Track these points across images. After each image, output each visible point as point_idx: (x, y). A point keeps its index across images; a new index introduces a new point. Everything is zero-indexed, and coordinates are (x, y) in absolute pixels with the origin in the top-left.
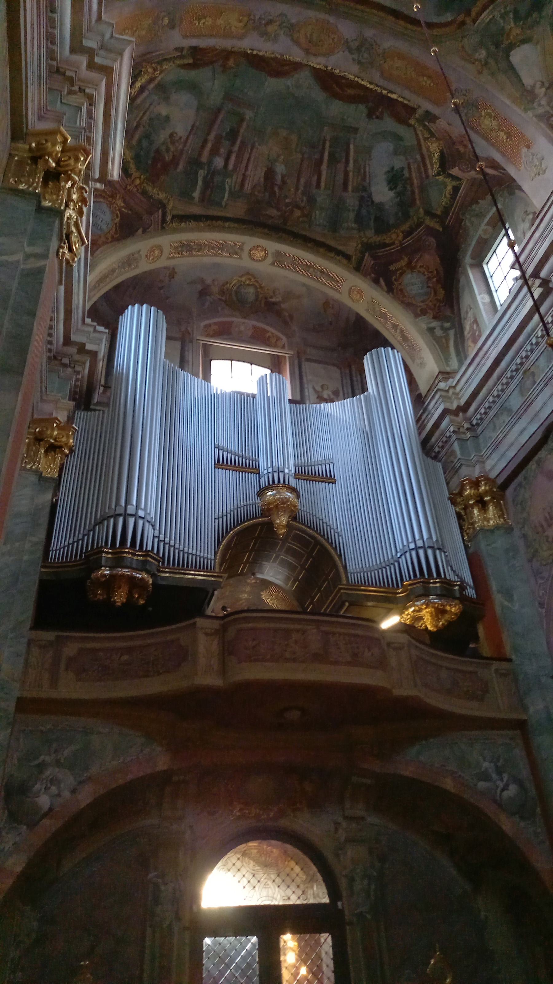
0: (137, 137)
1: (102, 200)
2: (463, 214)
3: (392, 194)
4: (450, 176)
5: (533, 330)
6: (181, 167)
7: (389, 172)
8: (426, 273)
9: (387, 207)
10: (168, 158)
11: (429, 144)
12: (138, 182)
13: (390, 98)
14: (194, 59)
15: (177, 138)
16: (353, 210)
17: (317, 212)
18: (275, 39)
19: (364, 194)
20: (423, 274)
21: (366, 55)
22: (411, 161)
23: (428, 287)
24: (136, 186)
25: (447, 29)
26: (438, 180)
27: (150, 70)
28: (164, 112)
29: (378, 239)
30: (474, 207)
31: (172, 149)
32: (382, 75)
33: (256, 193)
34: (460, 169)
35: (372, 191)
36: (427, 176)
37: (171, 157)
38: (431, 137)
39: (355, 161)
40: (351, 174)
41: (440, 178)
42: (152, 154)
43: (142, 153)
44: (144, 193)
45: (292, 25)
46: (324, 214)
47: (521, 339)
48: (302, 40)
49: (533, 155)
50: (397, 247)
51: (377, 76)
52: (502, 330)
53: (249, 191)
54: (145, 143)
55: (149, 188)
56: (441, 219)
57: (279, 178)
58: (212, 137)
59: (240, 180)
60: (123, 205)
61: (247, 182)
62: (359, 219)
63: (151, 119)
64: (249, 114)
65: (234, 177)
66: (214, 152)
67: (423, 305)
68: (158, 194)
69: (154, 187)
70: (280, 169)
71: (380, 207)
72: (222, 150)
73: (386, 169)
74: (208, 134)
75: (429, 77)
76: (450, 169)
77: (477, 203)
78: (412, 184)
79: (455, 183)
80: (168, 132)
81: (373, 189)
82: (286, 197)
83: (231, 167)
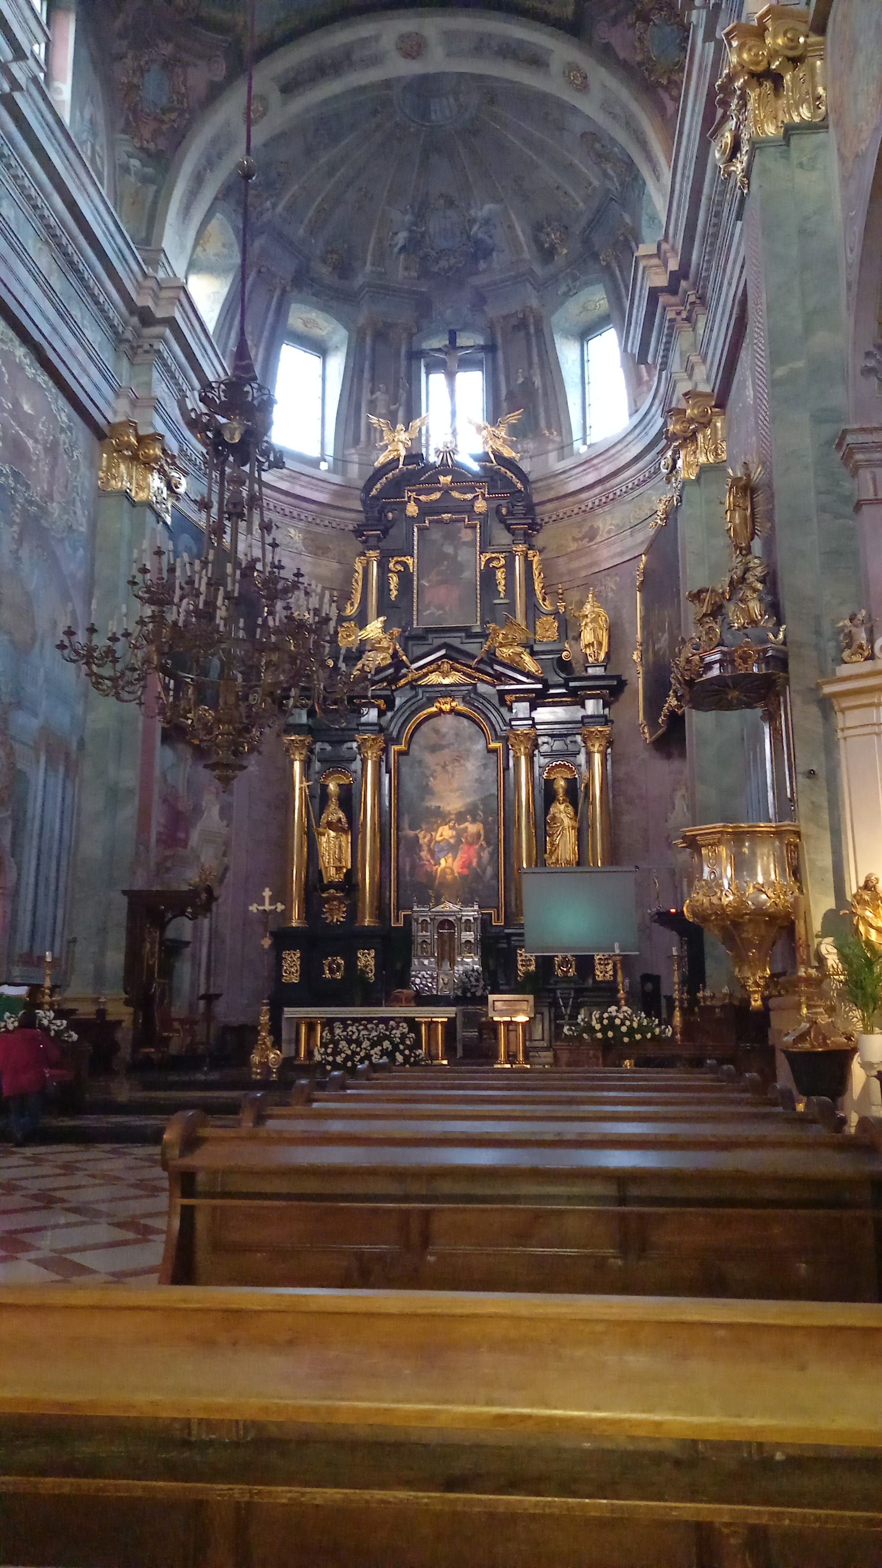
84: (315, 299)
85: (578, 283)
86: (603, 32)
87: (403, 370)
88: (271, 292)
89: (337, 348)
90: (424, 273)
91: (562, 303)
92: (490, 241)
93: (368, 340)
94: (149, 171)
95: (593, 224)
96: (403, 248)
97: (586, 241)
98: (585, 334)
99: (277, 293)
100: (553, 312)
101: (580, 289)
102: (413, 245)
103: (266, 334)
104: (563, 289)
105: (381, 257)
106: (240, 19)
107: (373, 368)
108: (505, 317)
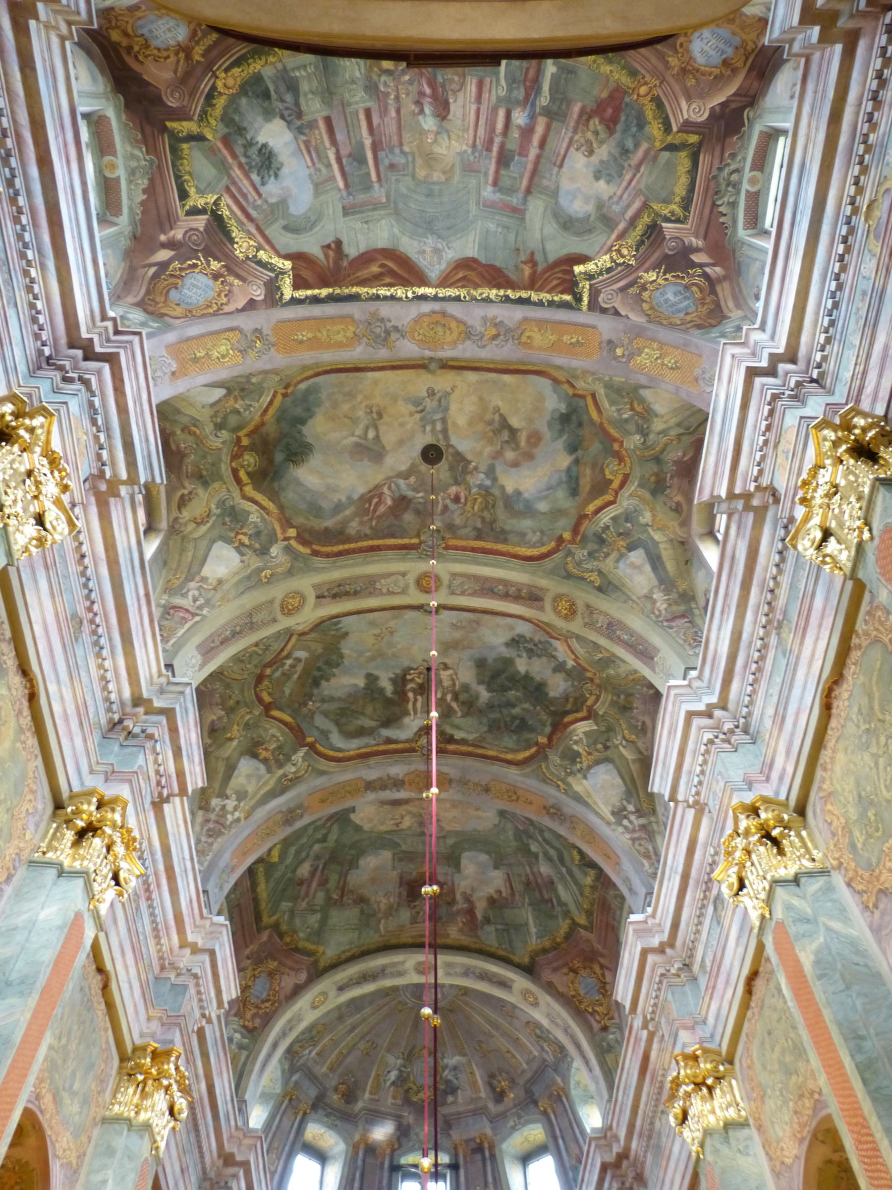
0: (640, 153)
1: (703, 68)
2: (151, 162)
3: (261, 139)
4: (203, 211)
5: (43, 267)
6: (576, 109)
7: (279, 169)
8: (156, 52)
9: (260, 119)
10: (595, 122)
11: (252, 243)
12: (643, 90)
13: (326, 285)
14: (572, 272)
15: (583, 148)
16: (305, 94)
17: (357, 74)
18: (485, 319)
19: (299, 123)
20: (159, 49)
21: (378, 330)
22: (259, 202)
23: (142, 35)
24: (646, 84)
25: (299, 378)
26: (213, 192)
27: (625, 252)
28: (602, 184)
29: (251, 68)
30: (146, 182)
31: (589, 135)
32: (351, 317)
33: (456, 78)
34: (197, 230)
35: (288, 131)
36: (228, 190)
37: (591, 122)
38: (255, 256)
39: (329, 166)
40: (327, 143)
41: (212, 199)
42: (619, 127)
43: (634, 129)
44: (633, 73)
45: (469, 338)
46: (347, 76)
47: (46, 238)
48: (453, 325)
49: (165, 374)
50: (218, 69)
51: (357, 315)
52: (77, 220)
53: (469, 78)
54: (629, 144)
55: (625, 80)
56: (176, 140)
57: (427, 110)
58: (533, 152)
59: (485, 95)
60: (670, 59)
61: (474, 94)
62: (293, 87)
63: (620, 175)
64: (488, 192)
65: (494, 99)
66: (527, 132)
67: (138, 14)
68: (611, 71)
69: (617, 82)
70: (429, 122)
71: (268, 114)
72: (515, 134)
73: (285, 171)
74: (539, 157)
75: (301, 342)
76: (208, 220)
77: (145, 191)
78: (241, 166)
79: (190, 203)
80: (595, 159)
81: (288, 136)
82: (411, 82)
83: (501, 113)
84: (326, 1119)
85: (522, 1121)
86: (547, 975)
87: (385, 1182)
88: (296, 1114)
89: (334, 1158)
90: (407, 1101)
91: (510, 1134)
92: (455, 1081)
93: (361, 1154)
94: (246, 1041)
95: (532, 1081)
96: (393, 1083)
97: (529, 1093)
98: (526, 1159)
99: (301, 1113)
100: (504, 1139)
101: (524, 1125)
102: (402, 1079)
103: (287, 1149)
104: (511, 1123)
105: (377, 1088)
106: (321, 949)
107: (362, 1176)
108: (467, 1141)
